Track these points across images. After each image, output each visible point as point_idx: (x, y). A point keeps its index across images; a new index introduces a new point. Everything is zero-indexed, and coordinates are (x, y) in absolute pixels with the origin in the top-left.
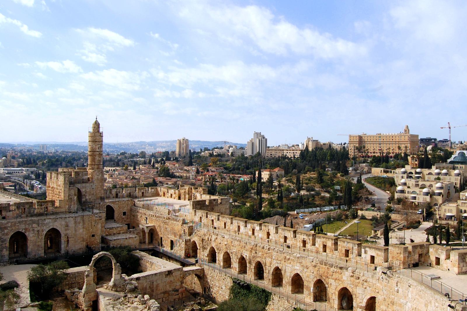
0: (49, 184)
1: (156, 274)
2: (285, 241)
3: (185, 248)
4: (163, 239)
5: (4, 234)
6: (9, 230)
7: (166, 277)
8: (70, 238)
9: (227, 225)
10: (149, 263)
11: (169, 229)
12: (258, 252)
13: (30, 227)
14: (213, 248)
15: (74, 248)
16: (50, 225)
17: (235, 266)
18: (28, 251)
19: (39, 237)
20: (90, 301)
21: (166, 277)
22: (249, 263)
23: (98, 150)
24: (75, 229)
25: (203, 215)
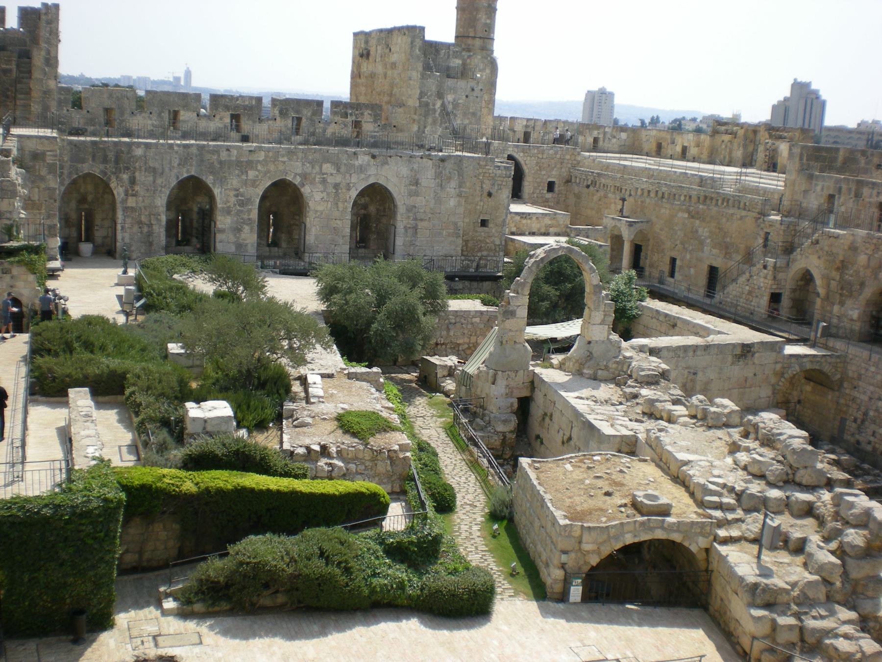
1: (707, 347)
3: (771, 288)
4: (678, 263)
5: (245, 183)
6: (257, 170)
7: (733, 364)
8: (422, 220)
10: (661, 318)
11: (704, 232)
13: (315, 171)
15: (428, 253)
16: (368, 173)
18: (307, 242)
19: (337, 204)
20: (512, 397)
21: (733, 364)
24: (436, 193)
25: (844, 187)
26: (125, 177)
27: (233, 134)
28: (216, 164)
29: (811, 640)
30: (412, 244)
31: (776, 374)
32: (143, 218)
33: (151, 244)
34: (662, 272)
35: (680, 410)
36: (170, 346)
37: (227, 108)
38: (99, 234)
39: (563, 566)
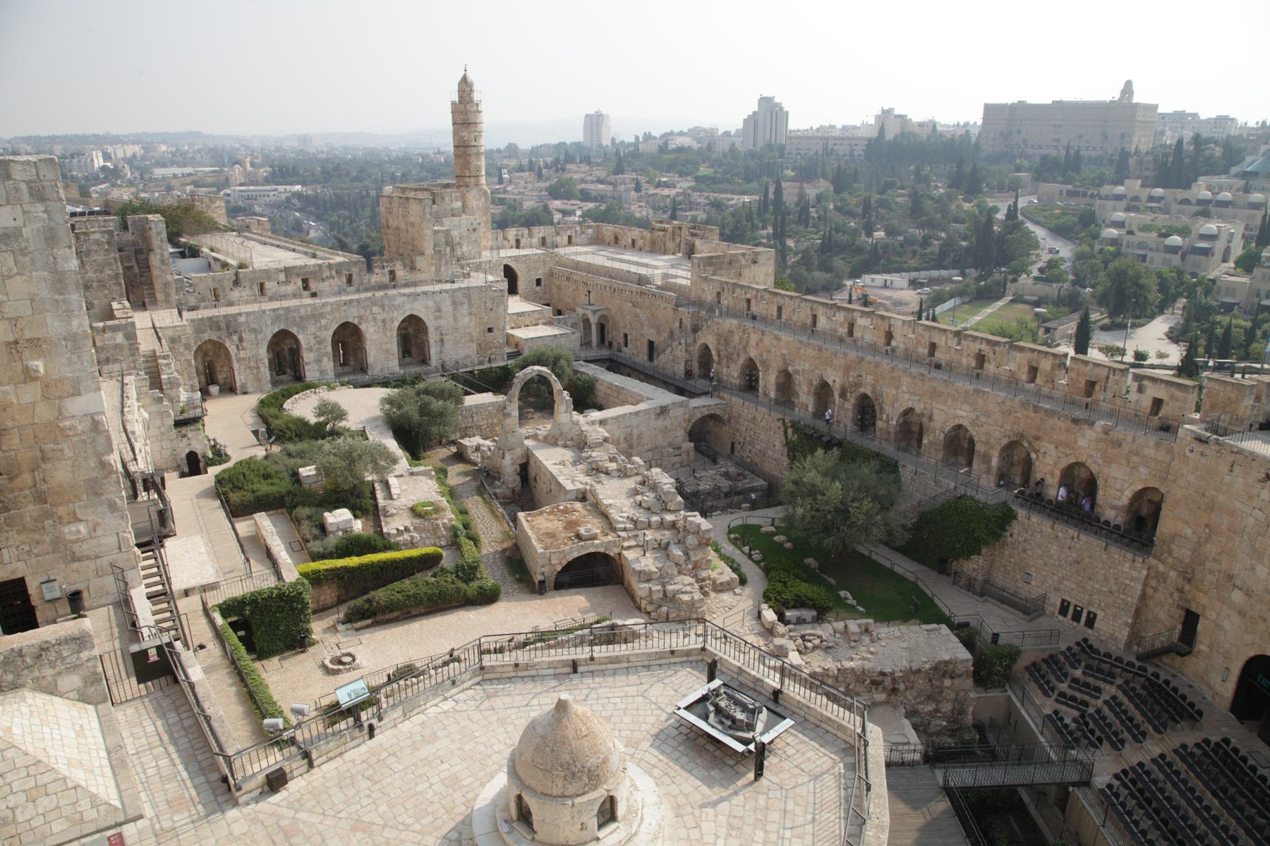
0: (387, 221)
1: (637, 413)
2: (932, 353)
4: (629, 337)
7: (656, 419)
9: (783, 311)
11: (643, 317)
12: (863, 374)
14: (751, 360)
15: (454, 357)
17: (805, 401)
21: (656, 419)
22: (840, 397)
23: (475, 144)
24: (454, 316)
26: (235, 338)
27: (306, 293)
28: (298, 319)
29: (669, 595)
30: (441, 352)
31: (685, 421)
32: (252, 364)
33: (260, 380)
34: (619, 344)
35: (613, 466)
36: (301, 470)
37: (298, 275)
38: (221, 377)
39: (543, 573)
